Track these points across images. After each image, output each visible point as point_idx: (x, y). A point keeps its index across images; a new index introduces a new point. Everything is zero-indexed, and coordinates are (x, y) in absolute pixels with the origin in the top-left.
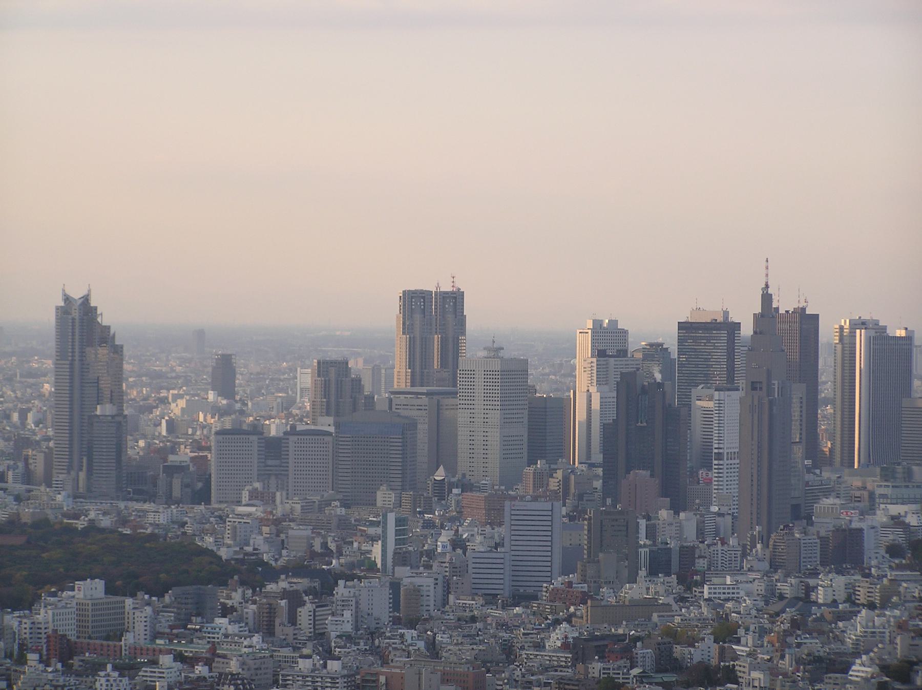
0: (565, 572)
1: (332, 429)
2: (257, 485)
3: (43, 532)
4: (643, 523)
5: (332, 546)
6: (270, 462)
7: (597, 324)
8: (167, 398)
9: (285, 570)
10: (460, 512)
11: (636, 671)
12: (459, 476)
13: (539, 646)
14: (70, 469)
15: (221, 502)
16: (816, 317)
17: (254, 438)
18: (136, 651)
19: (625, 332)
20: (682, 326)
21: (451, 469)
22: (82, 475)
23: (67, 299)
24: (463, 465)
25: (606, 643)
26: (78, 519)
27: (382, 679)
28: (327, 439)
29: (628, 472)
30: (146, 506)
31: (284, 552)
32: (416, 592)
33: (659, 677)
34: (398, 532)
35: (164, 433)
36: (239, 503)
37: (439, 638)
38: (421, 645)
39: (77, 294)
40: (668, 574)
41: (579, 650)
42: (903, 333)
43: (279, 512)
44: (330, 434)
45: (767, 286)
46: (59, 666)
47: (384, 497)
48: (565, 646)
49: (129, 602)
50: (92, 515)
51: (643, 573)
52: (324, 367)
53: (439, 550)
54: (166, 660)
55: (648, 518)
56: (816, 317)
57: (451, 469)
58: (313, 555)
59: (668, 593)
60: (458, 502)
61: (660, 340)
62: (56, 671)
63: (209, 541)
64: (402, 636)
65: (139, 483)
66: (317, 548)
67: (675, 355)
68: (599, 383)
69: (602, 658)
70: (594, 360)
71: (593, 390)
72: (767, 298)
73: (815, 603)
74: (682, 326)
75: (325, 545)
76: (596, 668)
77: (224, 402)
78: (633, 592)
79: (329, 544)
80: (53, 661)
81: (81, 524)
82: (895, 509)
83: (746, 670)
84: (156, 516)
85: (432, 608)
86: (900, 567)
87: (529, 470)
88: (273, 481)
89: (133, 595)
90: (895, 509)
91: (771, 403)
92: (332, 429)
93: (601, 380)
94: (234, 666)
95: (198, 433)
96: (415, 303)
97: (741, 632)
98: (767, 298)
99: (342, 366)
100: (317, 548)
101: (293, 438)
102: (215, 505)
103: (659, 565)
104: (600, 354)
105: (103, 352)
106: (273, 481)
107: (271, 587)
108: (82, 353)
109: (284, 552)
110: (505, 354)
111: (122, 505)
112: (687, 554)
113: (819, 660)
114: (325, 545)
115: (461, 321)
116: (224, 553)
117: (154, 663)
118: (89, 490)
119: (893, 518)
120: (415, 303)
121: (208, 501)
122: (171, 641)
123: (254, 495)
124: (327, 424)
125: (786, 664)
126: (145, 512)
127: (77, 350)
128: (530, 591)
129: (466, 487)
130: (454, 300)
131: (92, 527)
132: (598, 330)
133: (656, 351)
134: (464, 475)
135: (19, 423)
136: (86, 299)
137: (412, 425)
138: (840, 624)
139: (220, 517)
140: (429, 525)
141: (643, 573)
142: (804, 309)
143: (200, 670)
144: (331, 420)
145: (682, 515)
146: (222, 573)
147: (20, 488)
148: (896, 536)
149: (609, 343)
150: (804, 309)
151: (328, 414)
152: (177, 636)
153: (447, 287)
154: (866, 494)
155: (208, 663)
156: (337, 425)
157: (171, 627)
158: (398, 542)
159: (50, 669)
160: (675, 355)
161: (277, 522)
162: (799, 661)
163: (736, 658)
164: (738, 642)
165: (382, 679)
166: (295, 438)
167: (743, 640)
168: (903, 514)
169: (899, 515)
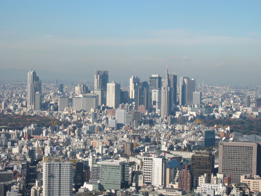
1: (82, 97)
7: (134, 77)
8: (50, 92)
10: (107, 113)
14: (31, 104)
15: (60, 111)
16: (176, 76)
19: (139, 79)
21: (105, 104)
22: (33, 106)
25: (135, 136)
27: (92, 143)
29: (140, 105)
35: (49, 99)
36: (64, 111)
37: (103, 136)
38: (99, 137)
42: (193, 79)
44: (82, 98)
53: (103, 120)
56: (176, 76)
58: (78, 120)
60: (106, 111)
61: (146, 81)
64: (96, 135)
65: (44, 106)
68: (134, 88)
73: (176, 130)
77: (61, 93)
79: (81, 119)
80: (27, 139)
81: (33, 115)
82: (191, 113)
83: (163, 142)
87: (120, 105)
92: (82, 97)
95: (56, 98)
97: (162, 135)
101: (74, 99)
102: (59, 111)
104: (134, 83)
105: (37, 82)
110: (117, 82)
113: (177, 140)
114: (80, 119)
116: (61, 120)
117: (47, 139)
118: (34, 108)
121: (58, 111)
123: (67, 109)
126: (45, 113)
127: (32, 84)
134: (108, 106)
135: (21, 97)
137: (98, 96)
138: (181, 134)
139: (60, 114)
140: (101, 115)
144: (82, 95)
151: (81, 94)
159: (26, 141)
165: (92, 143)
166: (75, 98)
167: (162, 136)
168: (193, 114)
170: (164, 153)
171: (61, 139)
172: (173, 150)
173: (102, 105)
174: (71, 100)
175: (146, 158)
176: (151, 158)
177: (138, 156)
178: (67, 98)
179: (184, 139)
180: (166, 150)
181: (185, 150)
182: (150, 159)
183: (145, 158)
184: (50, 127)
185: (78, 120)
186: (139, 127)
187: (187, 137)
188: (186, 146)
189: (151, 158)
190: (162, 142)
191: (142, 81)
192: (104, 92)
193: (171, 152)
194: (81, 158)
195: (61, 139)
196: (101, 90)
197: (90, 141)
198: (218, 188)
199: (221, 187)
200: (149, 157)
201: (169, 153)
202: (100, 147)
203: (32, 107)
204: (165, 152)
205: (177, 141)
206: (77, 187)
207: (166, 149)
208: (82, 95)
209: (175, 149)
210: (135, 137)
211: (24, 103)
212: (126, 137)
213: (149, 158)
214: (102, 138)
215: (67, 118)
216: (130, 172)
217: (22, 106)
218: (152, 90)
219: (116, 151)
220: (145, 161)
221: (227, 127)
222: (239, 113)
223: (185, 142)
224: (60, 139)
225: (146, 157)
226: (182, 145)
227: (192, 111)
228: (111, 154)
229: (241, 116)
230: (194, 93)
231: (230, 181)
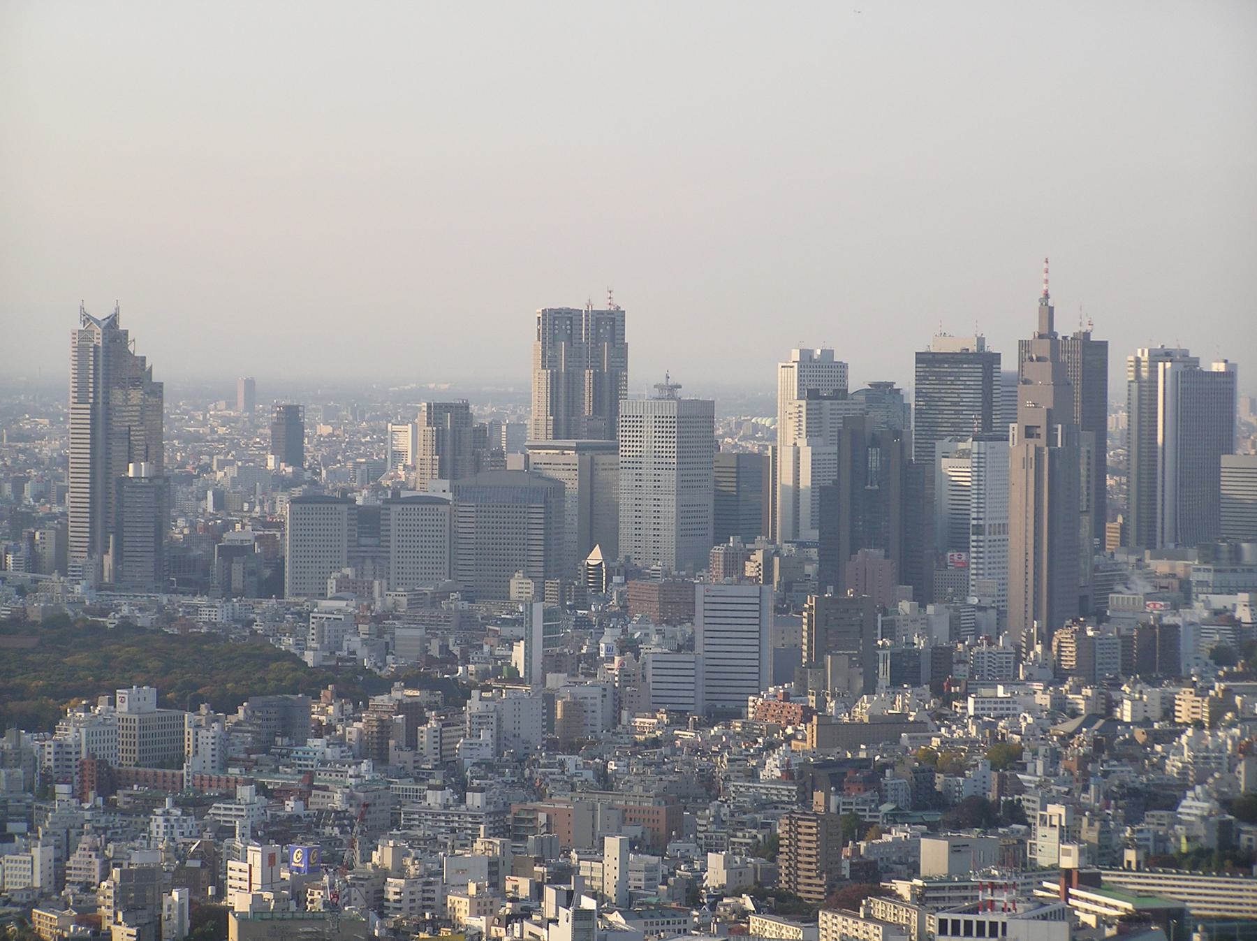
1: (449, 496)
2: (347, 571)
3: (62, 631)
5: (456, 650)
6: (364, 541)
7: (806, 355)
8: (210, 466)
9: (396, 677)
10: (625, 607)
11: (886, 808)
12: (621, 559)
13: (753, 775)
14: (91, 550)
15: (298, 595)
16: (1103, 346)
17: (343, 508)
19: (844, 366)
20: (921, 358)
22: (108, 560)
23: (87, 319)
24: (626, 545)
25: (844, 770)
26: (106, 616)
27: (542, 818)
28: (442, 508)
29: (854, 551)
30: (197, 600)
31: (389, 658)
34: (547, 629)
35: (210, 509)
36: (323, 596)
37: (612, 766)
38: (589, 774)
39: (101, 314)
42: (1219, 367)
43: (378, 606)
44: (445, 502)
45: (1047, 296)
46: (100, 801)
47: (519, 586)
48: (788, 774)
50: (125, 610)
52: (436, 412)
53: (602, 654)
54: (244, 792)
55: (885, 613)
56: (1103, 346)
57: (610, 552)
60: (620, 595)
62: (94, 808)
63: (288, 642)
64: (562, 764)
65: (184, 571)
66: (434, 650)
67: (911, 399)
68: (809, 434)
70: (803, 403)
71: (802, 443)
72: (1048, 313)
73: (1121, 722)
74: (921, 358)
75: (444, 648)
77: (289, 470)
79: (451, 648)
80: (91, 795)
81: (111, 622)
82: (1220, 601)
83: (1037, 806)
84: (210, 612)
85: (599, 728)
87: (718, 550)
88: (369, 565)
89: (195, 709)
90: (1220, 601)
91: (1052, 455)
92: (449, 496)
93: (814, 430)
94: (337, 801)
95: (258, 509)
96: (559, 326)
97: (1027, 756)
98: (1048, 313)
99: (461, 411)
100: (434, 650)
102: (289, 598)
103: (905, 671)
104: (811, 395)
105: (136, 395)
106: (369, 565)
107: (380, 700)
108: (107, 393)
109: (389, 658)
110: (684, 394)
111: (165, 599)
114: (444, 648)
115: (620, 351)
116: (309, 658)
117: (229, 797)
119: (1217, 613)
120: (559, 326)
121: (281, 595)
122: (248, 770)
123: (343, 584)
124: (441, 488)
125: (1089, 798)
126: (196, 608)
128: (731, 706)
129: (632, 573)
130: (610, 325)
131: (126, 626)
132: (807, 363)
133: (883, 392)
134: (628, 558)
135: (12, 498)
136: (112, 321)
138: (1158, 748)
139: (299, 614)
140: (582, 623)
142: (1087, 335)
143: (290, 805)
144: (446, 484)
145: (930, 609)
149: (821, 381)
150: (1087, 335)
151: (441, 476)
152: (256, 763)
153: (601, 305)
154: (1176, 583)
155: (303, 796)
156: (454, 489)
157: (249, 752)
158: (547, 643)
159: (87, 806)
160: (911, 399)
161: (378, 619)
162: (1108, 796)
163: (1021, 789)
164: (1023, 769)
165: (542, 818)
166: (399, 508)
167: (1030, 767)
168: (1229, 607)
169: (1225, 609)
170: (1057, 887)
171: (325, 789)
172: (1116, 862)
175: (956, 923)
176: (987, 917)
178: (340, 507)
179: (1182, 786)
180: (1069, 862)
181: (1198, 861)
182: (981, 924)
183: (943, 923)
184: (241, 711)
186: (863, 710)
187: (1203, 767)
188: (1201, 831)
189: (987, 917)
190: (1029, 802)
191: (857, 381)
192: (602, 459)
193: (1108, 877)
194: (480, 923)
195: (325, 789)
196: (578, 449)
197: (530, 805)
200: (975, 911)
201: (1091, 882)
202: (612, 845)
207: (1068, 853)
209: (1130, 855)
210: (845, 774)
212: (778, 773)
213: (974, 918)
215: (353, 643)
218: (938, 443)
224: (318, 788)
225: (949, 917)
226: (1171, 826)
227: (1220, 589)
230: (1226, 460)
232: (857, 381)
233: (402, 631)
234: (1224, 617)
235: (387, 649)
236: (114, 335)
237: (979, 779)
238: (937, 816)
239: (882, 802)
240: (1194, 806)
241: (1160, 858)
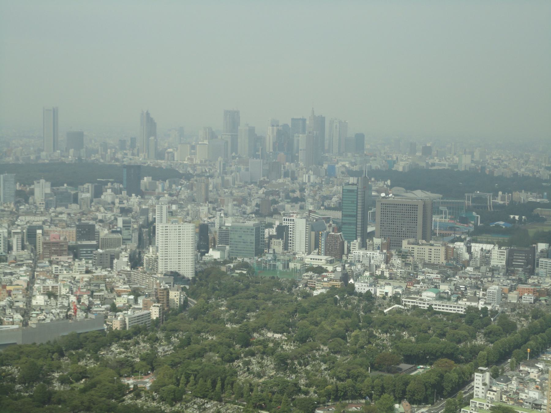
0: (264, 176)
4: (282, 166)
5: (207, 170)
6: (192, 151)
11: (280, 199)
13: (257, 193)
16: (324, 118)
17: (188, 145)
18: (159, 193)
21: (236, 153)
22: (146, 154)
32: (228, 180)
33: (286, 200)
40: (288, 177)
41: (267, 194)
48: (263, 193)
49: (157, 182)
51: (282, 177)
54: (166, 195)
56: (324, 118)
57: (236, 153)
58: (202, 172)
59: (288, 181)
63: (177, 169)
65: (160, 155)
66: (204, 171)
67: (290, 127)
69: (272, 195)
72: (313, 112)
75: (206, 170)
76: (271, 198)
78: (281, 181)
81: (146, 165)
82: (343, 163)
86: (344, 176)
90: (343, 163)
94: (183, 197)
98: (313, 112)
100: (204, 171)
101: (198, 145)
103: (286, 175)
107: (192, 179)
112: (293, 172)
113: (325, 197)
116: (181, 172)
117: (164, 196)
118: (148, 157)
123: (188, 159)
125: (317, 197)
131: (149, 166)
133: (286, 126)
141: (282, 177)
146: (180, 176)
147: (131, 157)
148: (343, 169)
155: (177, 196)
160: (290, 127)
161: (194, 165)
162: (320, 197)
163: (304, 196)
173: (232, 153)
174: (193, 147)
176: (292, 218)
177: (275, 216)
185: (202, 172)
191: (280, 124)
198: (375, 255)
199: (378, 255)
201: (314, 212)
203: (145, 155)
204: (310, 211)
205: (326, 198)
206: (203, 254)
208: (207, 141)
211: (135, 151)
214: (232, 194)
215: (189, 169)
216: (267, 236)
217: (133, 154)
219: (249, 209)
220: (285, 222)
221: (387, 181)
222: (402, 164)
223: (335, 199)
228: (244, 213)
229: (404, 167)
231: (389, 249)
232: (280, 124)
233: (198, 167)
234: (344, 166)
235: (195, 170)
236: (148, 114)
237: (297, 194)
238: (289, 200)
239: (280, 198)
240: (335, 199)
241: (328, 208)
